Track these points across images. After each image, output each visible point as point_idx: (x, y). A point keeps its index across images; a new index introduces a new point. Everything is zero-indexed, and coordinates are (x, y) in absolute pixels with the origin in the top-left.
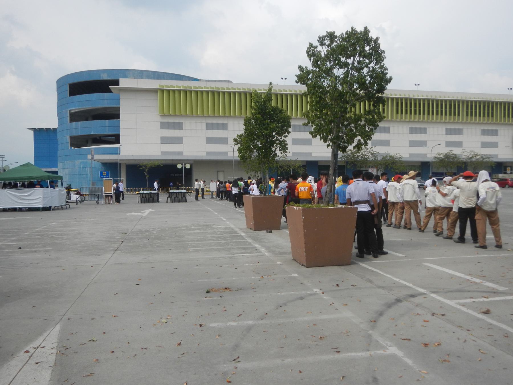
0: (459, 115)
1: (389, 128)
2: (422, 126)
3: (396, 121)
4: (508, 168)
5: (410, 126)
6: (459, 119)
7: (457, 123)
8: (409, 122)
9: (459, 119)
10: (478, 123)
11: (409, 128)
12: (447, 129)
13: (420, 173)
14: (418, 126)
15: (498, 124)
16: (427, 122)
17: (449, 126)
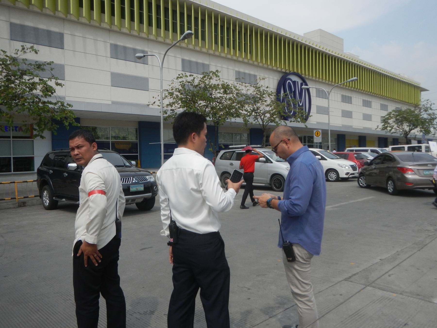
0: (203, 38)
1: (61, 36)
2: (139, 46)
3: (77, 23)
4: (315, 131)
5: (112, 42)
6: (204, 45)
7: (200, 52)
8: (110, 31)
9: (204, 45)
10: (231, 60)
11: (111, 45)
12: (183, 60)
13: (137, 144)
14: (130, 44)
15: (257, 66)
16: (148, 40)
17: (188, 57)
